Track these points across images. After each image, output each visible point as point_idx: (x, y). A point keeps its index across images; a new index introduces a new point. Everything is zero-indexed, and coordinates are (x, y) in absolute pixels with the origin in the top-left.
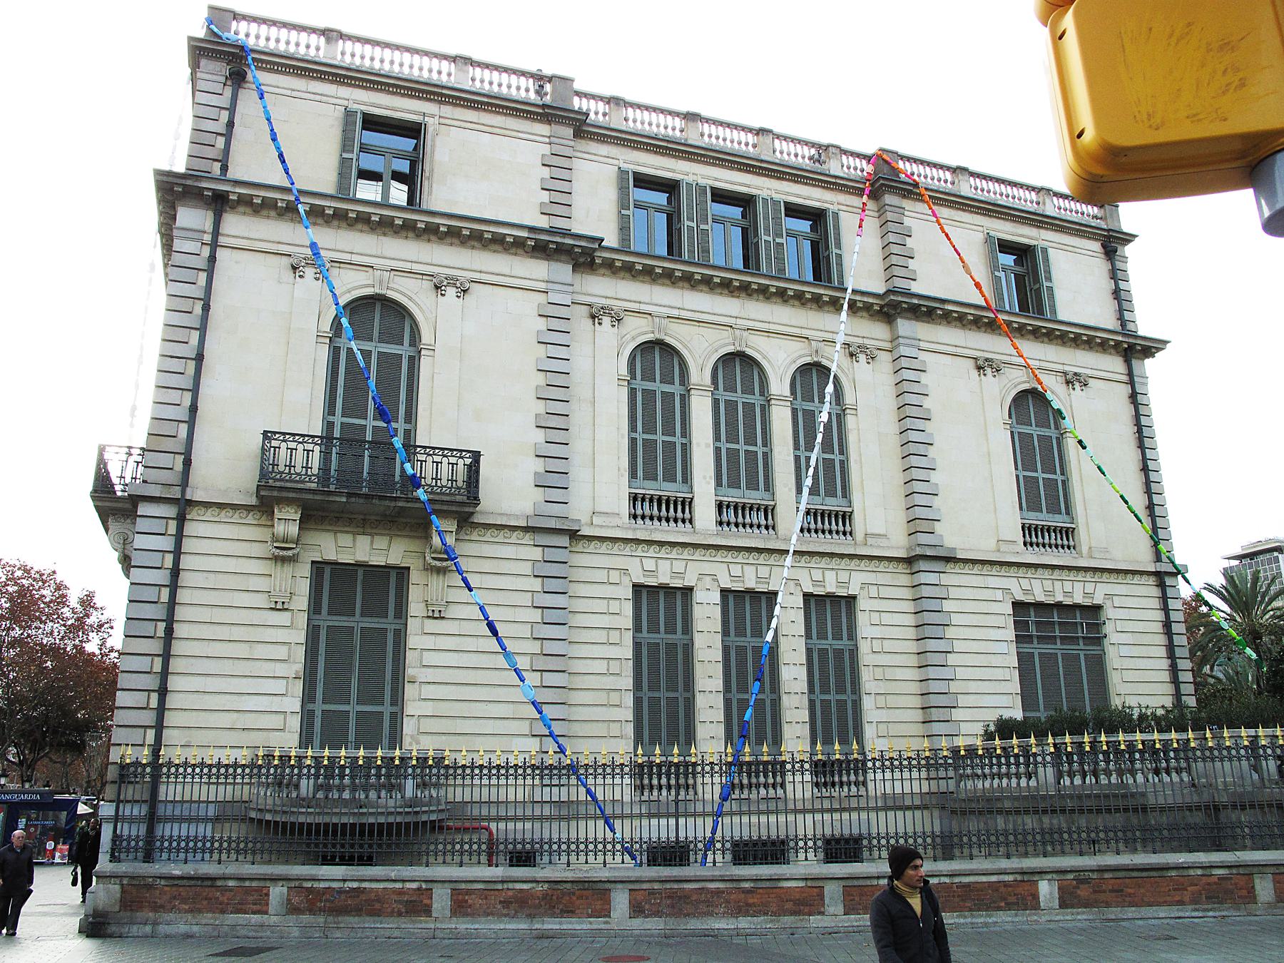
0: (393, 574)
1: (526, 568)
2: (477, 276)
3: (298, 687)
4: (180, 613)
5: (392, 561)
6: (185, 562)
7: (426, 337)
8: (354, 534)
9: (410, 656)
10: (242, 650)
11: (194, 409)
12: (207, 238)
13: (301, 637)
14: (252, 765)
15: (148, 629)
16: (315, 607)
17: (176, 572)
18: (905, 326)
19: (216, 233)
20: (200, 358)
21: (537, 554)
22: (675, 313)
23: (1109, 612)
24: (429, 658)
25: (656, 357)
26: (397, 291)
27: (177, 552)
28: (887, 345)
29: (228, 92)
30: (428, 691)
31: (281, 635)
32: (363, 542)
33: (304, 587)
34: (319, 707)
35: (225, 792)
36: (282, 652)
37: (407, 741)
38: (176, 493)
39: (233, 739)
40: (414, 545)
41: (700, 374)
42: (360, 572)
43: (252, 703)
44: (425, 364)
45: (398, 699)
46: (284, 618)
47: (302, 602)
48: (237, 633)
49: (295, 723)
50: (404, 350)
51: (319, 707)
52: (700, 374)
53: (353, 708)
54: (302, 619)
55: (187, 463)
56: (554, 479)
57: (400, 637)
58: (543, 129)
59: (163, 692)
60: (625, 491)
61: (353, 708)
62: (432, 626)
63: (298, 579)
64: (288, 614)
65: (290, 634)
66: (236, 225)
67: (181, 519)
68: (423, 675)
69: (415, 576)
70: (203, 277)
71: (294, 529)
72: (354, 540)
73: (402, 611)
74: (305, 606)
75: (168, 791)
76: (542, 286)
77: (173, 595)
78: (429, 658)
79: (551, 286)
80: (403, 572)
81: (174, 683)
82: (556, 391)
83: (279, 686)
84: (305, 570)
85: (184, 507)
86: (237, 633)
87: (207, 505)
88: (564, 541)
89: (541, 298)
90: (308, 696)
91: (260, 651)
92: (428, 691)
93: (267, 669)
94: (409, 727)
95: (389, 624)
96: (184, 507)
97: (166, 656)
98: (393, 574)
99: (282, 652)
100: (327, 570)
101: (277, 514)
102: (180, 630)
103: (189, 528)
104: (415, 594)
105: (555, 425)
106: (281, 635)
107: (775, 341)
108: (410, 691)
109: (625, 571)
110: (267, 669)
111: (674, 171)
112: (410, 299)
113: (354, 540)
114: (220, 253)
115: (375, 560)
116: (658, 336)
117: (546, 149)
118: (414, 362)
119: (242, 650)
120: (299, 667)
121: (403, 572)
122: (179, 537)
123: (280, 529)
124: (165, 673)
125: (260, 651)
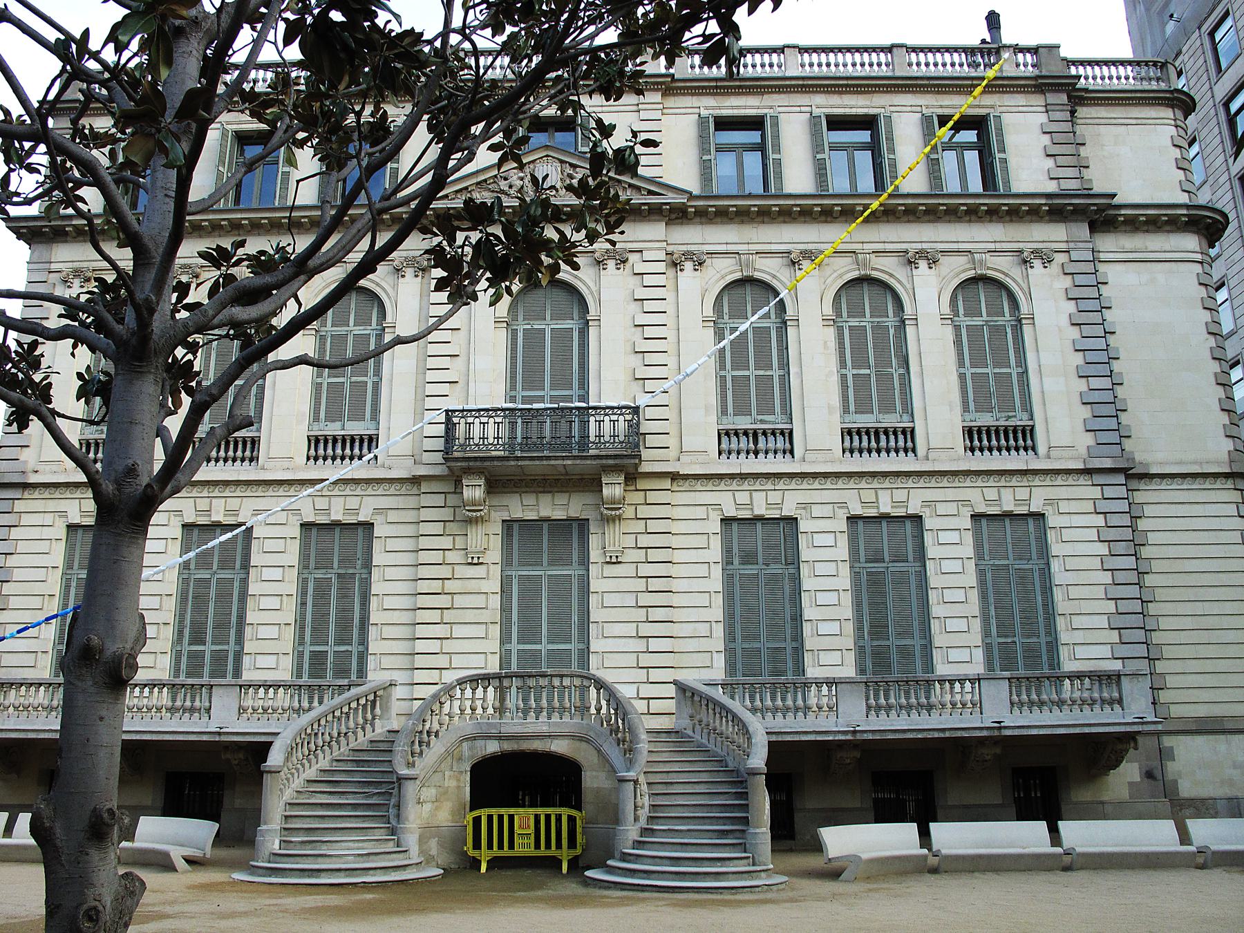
0: (575, 525)
3: (495, 631)
5: (573, 513)
8: (537, 492)
16: (507, 561)
24: (610, 600)
32: (545, 499)
33: (496, 543)
34: (515, 646)
40: (589, 498)
42: (545, 525)
53: (544, 647)
54: (496, 571)
61: (544, 647)
64: (484, 567)
71: (479, 493)
74: (498, 560)
78: (610, 600)
80: (583, 524)
95: (574, 571)
98: (575, 525)
100: (516, 526)
101: (465, 482)
104: (594, 541)
115: (559, 514)
121: (583, 524)
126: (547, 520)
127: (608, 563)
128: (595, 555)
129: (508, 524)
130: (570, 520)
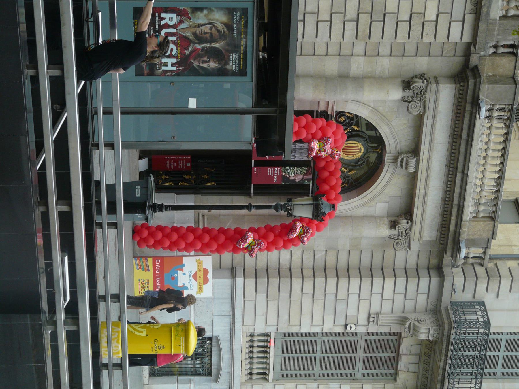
63: (389, 327)
72: (416, 354)
84: (395, 329)
100: (396, 338)
113: (416, 354)
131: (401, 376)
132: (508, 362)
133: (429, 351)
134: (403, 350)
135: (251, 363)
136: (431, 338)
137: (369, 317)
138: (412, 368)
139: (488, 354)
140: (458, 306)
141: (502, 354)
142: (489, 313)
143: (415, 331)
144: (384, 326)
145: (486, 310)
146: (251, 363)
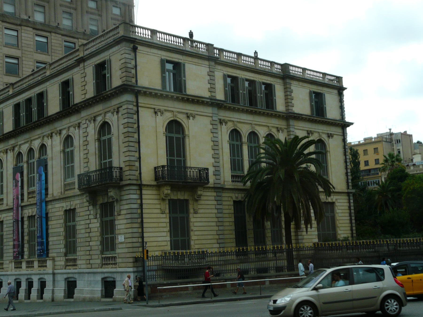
1: (213, 198)
2: (197, 113)
4: (144, 216)
6: (144, 201)
7: (187, 132)
9: (191, 224)
10: (156, 225)
11: (140, 158)
12: (135, 104)
13: (168, 220)
14: (161, 256)
15: (136, 221)
16: (170, 213)
17: (141, 205)
18: (292, 122)
19: (137, 102)
20: (139, 142)
21: (215, 194)
22: (239, 120)
23: (337, 204)
24: (196, 224)
25: (235, 134)
26: (179, 118)
27: (141, 199)
28: (286, 127)
29: (133, 54)
30: (196, 233)
31: (164, 220)
32: (179, 193)
35: (157, 263)
36: (164, 225)
37: (192, 247)
38: (139, 182)
39: (156, 249)
41: (245, 139)
43: (160, 239)
44: (187, 140)
45: (189, 236)
46: (164, 216)
47: (167, 211)
48: (155, 220)
49: (169, 243)
50: (180, 136)
51: (173, 239)
52: (245, 139)
55: (140, 173)
56: (217, 173)
57: (188, 218)
58: (207, 63)
59: (143, 237)
60: (230, 174)
62: (195, 215)
65: (165, 220)
66: (142, 100)
67: (141, 190)
68: (195, 229)
69: (191, 202)
70: (135, 117)
73: (188, 212)
74: (168, 212)
75: (147, 263)
76: (211, 115)
77: (142, 211)
78: (196, 224)
79: (213, 115)
81: (145, 235)
82: (216, 145)
83: (165, 234)
85: (141, 187)
86: (155, 220)
87: (145, 185)
88: (220, 190)
89: (210, 119)
90: (171, 237)
91: (161, 225)
92: (196, 233)
93: (162, 229)
94: (192, 243)
96: (141, 187)
97: (142, 228)
99: (164, 225)
102: (145, 220)
103: (144, 192)
105: (216, 157)
106: (164, 220)
107: (261, 127)
108: (192, 233)
109: (232, 197)
110: (162, 229)
111: (236, 74)
112: (182, 121)
114: (139, 108)
115: (182, 198)
116: (235, 128)
117: (208, 70)
118: (184, 138)
119: (156, 225)
120: (169, 228)
121: (187, 201)
122: (141, 194)
123: (166, 192)
124: (143, 232)
125: (161, 225)
126: (179, 200)
127: (194, 213)
128: (191, 211)
129: (169, 200)
130: (184, 200)
131: (186, 197)
132: (179, 155)
133: (175, 187)
134: (175, 198)
135: (110, 264)
136: (170, 188)
137: (163, 213)
138: (183, 194)
139: (176, 165)
140: (157, 178)
141: (176, 158)
142: (159, 165)
143: (167, 195)
144: (166, 207)
145: (158, 167)
146: (110, 264)
